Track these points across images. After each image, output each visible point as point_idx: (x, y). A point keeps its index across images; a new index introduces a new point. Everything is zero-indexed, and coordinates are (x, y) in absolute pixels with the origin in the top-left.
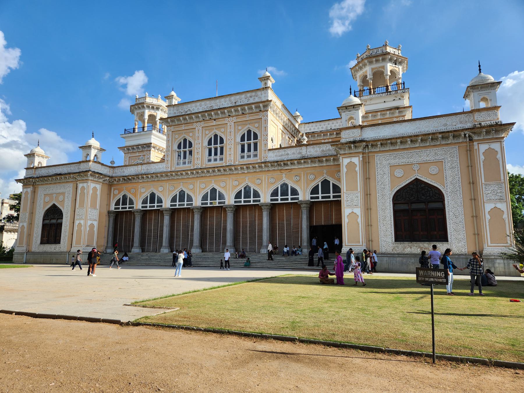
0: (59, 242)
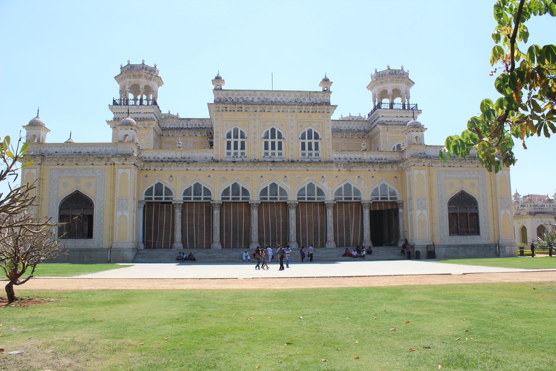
0: (90, 235)
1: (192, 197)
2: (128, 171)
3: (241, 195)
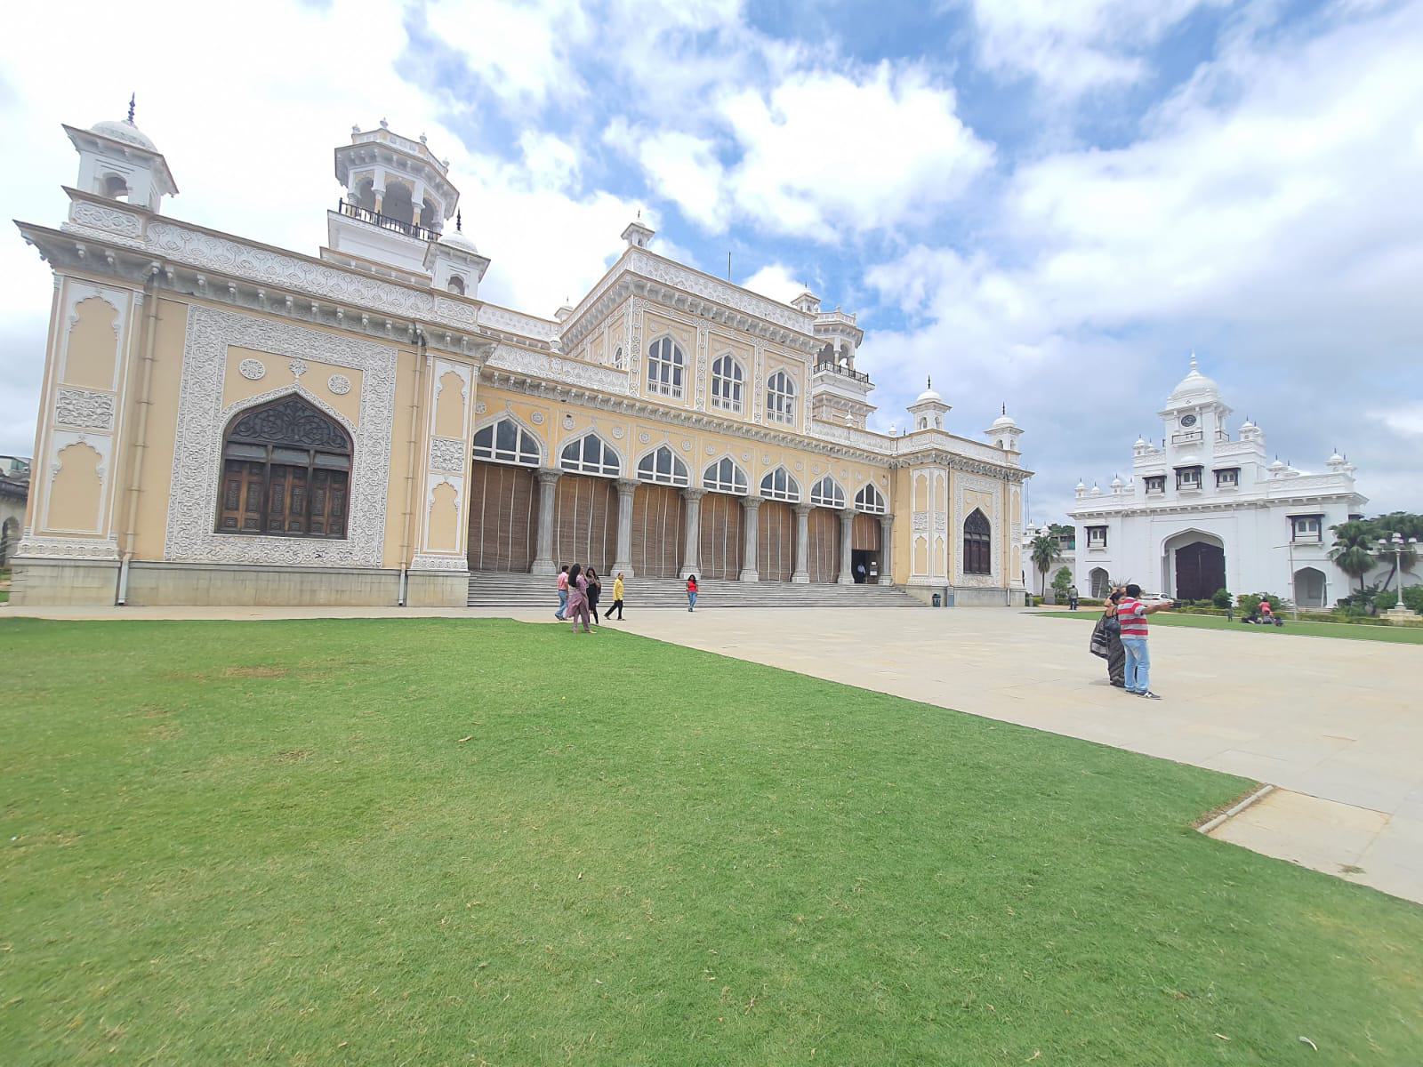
0: (338, 529)
1: (581, 463)
3: (672, 472)
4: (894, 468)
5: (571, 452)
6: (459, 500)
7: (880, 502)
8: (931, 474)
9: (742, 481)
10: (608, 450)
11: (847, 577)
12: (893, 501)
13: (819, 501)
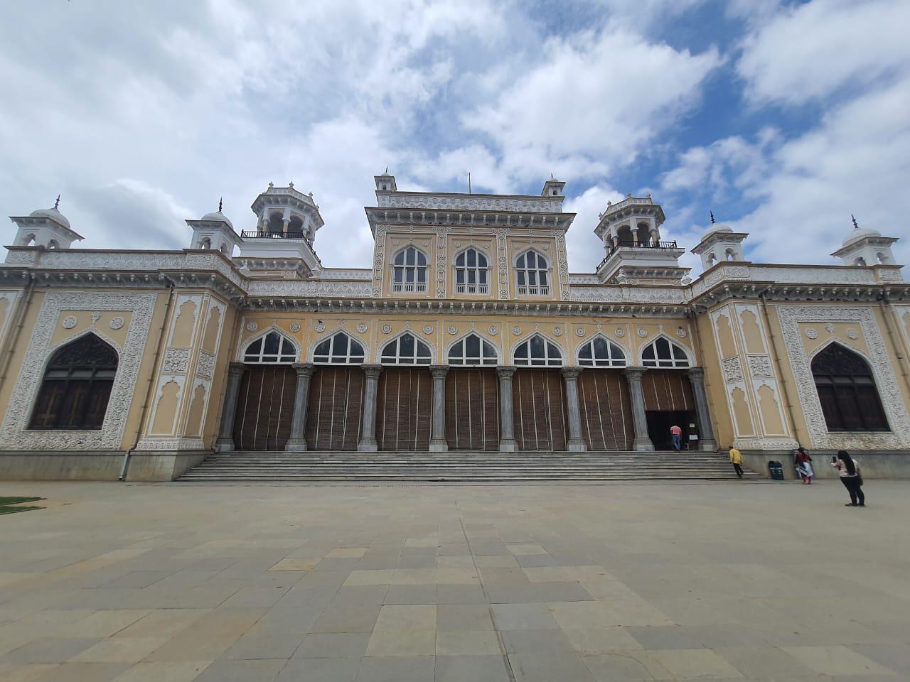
0: (97, 423)
2: (197, 299)
4: (693, 315)
5: (323, 349)
6: (179, 394)
7: (679, 353)
8: (733, 313)
9: (492, 354)
10: (354, 344)
11: (644, 445)
12: (700, 353)
13: (591, 363)
